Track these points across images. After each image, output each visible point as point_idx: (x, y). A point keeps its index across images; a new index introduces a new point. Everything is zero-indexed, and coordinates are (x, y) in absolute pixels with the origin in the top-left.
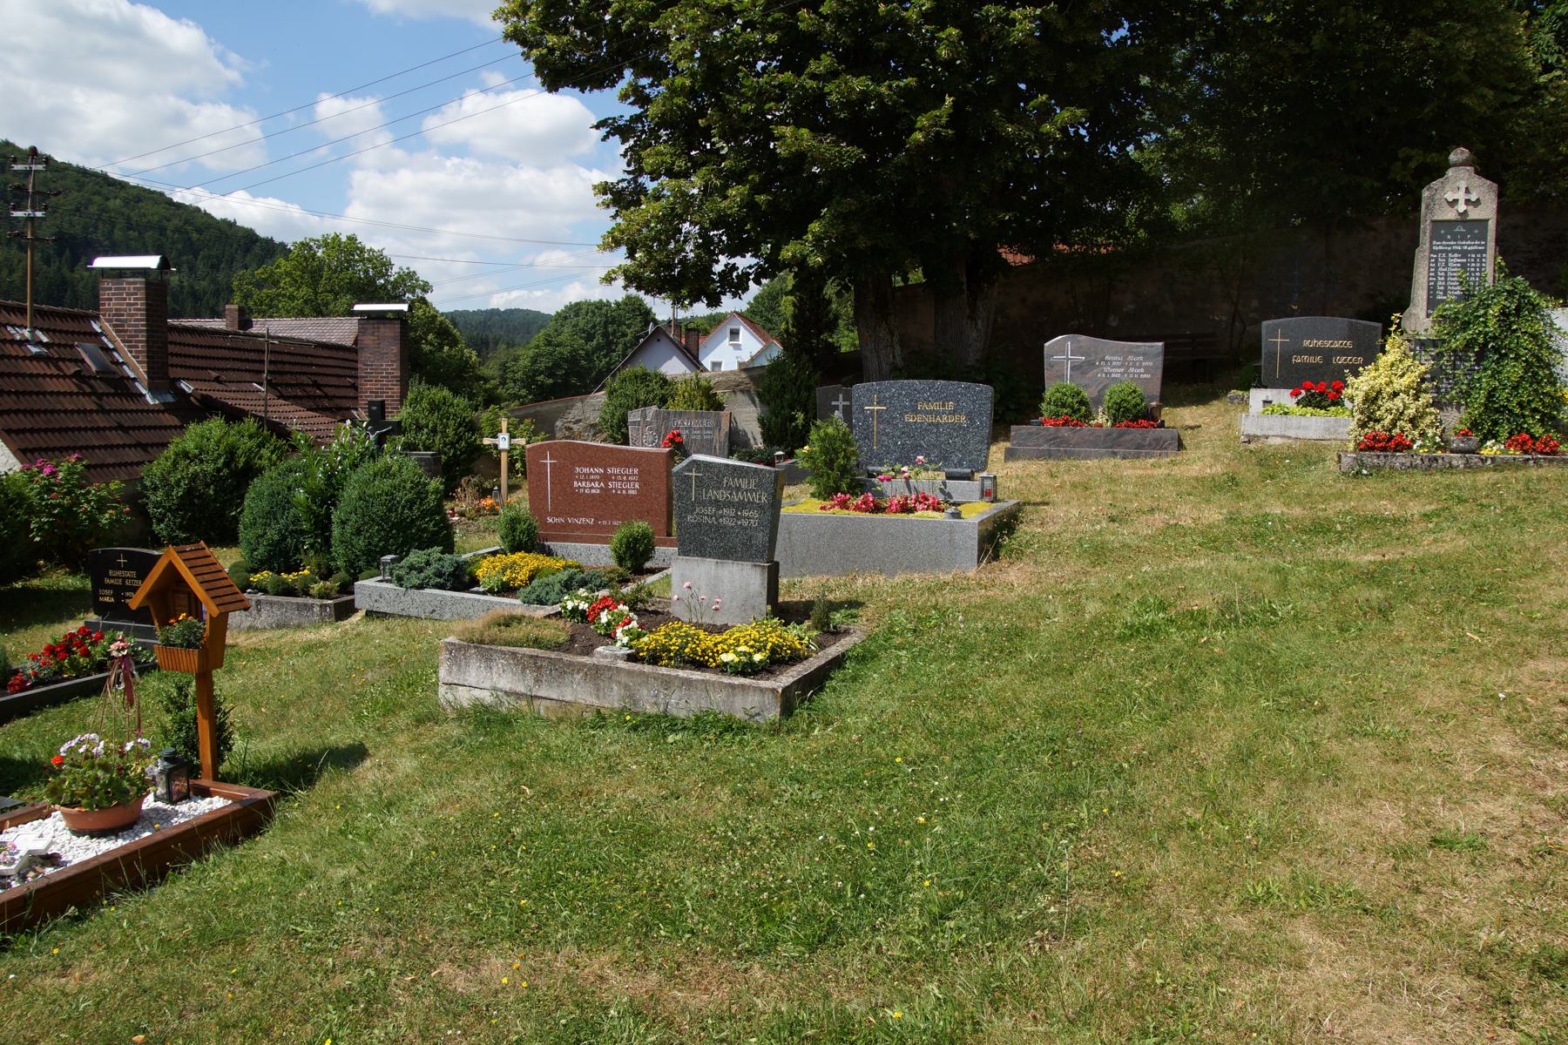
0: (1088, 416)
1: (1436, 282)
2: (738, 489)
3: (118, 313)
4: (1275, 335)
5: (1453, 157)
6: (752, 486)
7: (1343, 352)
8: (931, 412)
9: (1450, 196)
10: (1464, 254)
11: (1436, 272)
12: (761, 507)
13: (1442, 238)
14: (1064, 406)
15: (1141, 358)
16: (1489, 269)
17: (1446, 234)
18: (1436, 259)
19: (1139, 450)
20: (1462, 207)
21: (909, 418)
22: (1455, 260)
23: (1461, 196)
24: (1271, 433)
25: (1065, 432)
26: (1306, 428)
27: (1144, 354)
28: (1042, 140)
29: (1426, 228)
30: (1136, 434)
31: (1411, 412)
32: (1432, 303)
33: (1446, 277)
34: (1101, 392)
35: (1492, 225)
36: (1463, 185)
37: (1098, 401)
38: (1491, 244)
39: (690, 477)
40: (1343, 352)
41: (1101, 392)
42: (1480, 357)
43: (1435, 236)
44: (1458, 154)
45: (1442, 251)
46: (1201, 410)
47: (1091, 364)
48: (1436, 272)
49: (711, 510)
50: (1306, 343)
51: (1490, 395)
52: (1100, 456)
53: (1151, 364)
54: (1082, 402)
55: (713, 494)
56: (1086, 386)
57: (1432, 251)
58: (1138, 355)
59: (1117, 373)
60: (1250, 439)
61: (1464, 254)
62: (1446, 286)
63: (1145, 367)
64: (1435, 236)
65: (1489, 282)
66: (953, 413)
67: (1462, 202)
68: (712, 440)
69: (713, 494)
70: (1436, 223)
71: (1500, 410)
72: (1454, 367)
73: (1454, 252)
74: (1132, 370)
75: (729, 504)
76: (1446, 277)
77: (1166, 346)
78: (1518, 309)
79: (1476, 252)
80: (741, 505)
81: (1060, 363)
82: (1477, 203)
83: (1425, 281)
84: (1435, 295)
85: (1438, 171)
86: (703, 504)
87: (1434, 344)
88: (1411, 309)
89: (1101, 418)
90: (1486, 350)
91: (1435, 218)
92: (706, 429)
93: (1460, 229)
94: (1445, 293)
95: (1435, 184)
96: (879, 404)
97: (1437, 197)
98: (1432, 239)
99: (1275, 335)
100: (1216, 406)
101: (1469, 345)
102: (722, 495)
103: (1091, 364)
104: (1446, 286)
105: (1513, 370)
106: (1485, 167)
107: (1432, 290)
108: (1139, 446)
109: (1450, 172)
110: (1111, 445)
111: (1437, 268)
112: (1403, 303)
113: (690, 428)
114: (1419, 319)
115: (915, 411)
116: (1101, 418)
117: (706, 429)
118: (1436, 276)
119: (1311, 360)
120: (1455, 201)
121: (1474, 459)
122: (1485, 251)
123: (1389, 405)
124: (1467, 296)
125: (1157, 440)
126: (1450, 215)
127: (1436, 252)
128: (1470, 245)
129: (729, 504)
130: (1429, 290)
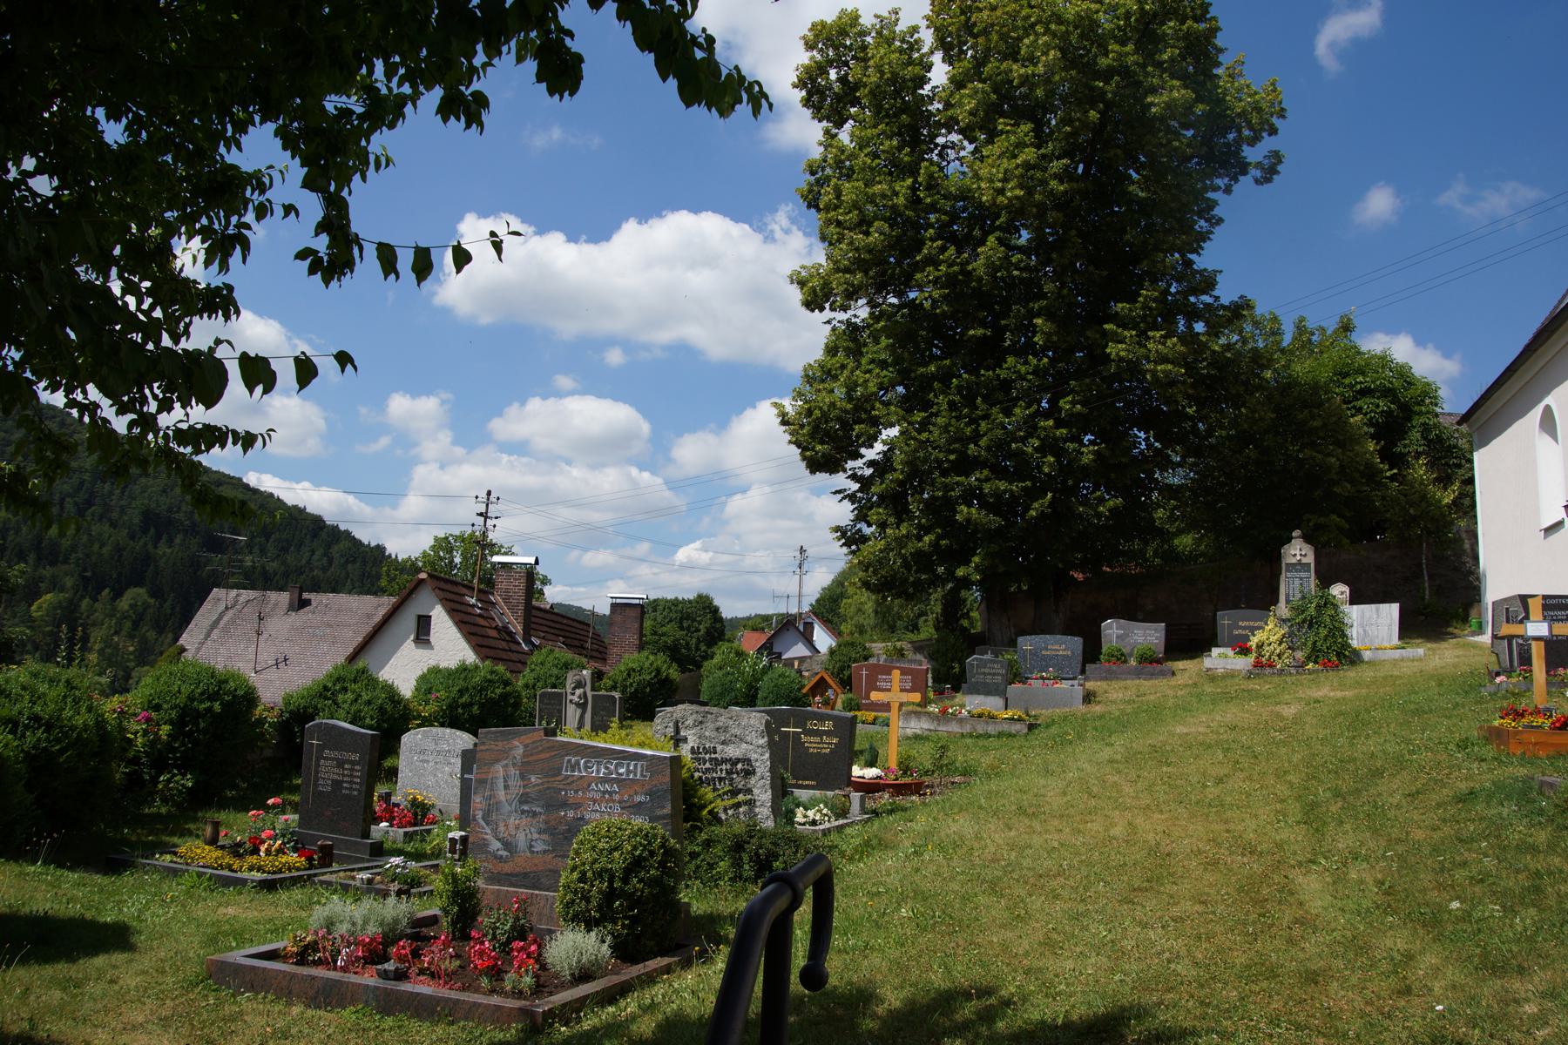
0: (1125, 662)
3: (507, 591)
4: (1224, 619)
5: (1294, 534)
10: (1301, 579)
14: (1113, 656)
16: (1313, 586)
19: (1152, 675)
20: (1298, 558)
21: (1043, 652)
22: (1297, 582)
23: (1298, 552)
25: (1114, 668)
27: (1155, 630)
28: (1099, 515)
29: (1283, 565)
30: (1149, 668)
31: (1278, 651)
32: (1288, 601)
34: (1132, 650)
35: (1313, 566)
37: (1131, 655)
38: (1313, 575)
41: (1132, 650)
42: (1310, 627)
43: (1287, 571)
44: (1296, 533)
46: (1189, 662)
47: (1127, 635)
49: (982, 677)
50: (1240, 623)
51: (1315, 643)
52: (1133, 679)
54: (1122, 655)
55: (983, 670)
56: (1125, 647)
58: (1150, 630)
59: (1140, 640)
60: (1208, 670)
61: (1301, 579)
64: (1287, 571)
65: (1313, 593)
69: (983, 670)
71: (1319, 651)
72: (1299, 631)
75: (990, 674)
77: (1166, 626)
78: (1325, 604)
80: (994, 674)
81: (1110, 635)
82: (1305, 555)
85: (1289, 540)
87: (1289, 620)
88: (1279, 605)
89: (1133, 662)
90: (1311, 623)
95: (1286, 547)
99: (1224, 619)
100: (1196, 661)
101: (1304, 621)
102: (987, 671)
103: (1127, 635)
105: (1323, 632)
106: (1307, 538)
107: (1287, 596)
108: (1152, 674)
110: (1138, 674)
112: (1276, 601)
114: (1282, 609)
115: (1047, 650)
116: (1133, 662)
120: (1295, 555)
121: (1300, 670)
123: (1267, 648)
124: (1303, 598)
125: (1161, 671)
126: (1293, 561)
128: (1303, 575)
129: (990, 674)
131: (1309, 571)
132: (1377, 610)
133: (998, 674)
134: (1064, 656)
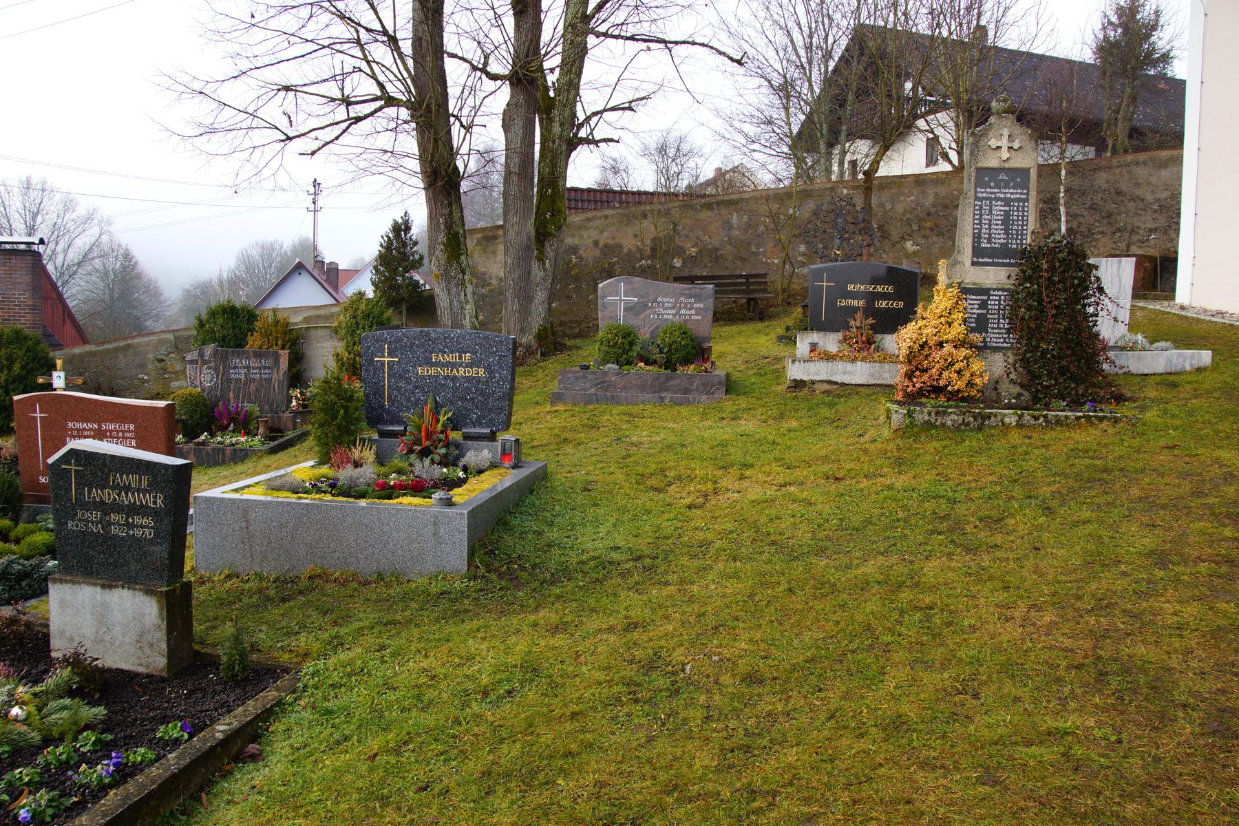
1: (980, 230)
2: (127, 489)
6: (144, 484)
7: (884, 296)
8: (448, 364)
9: (993, 143)
10: (1007, 202)
11: (980, 219)
12: (155, 513)
15: (693, 300)
17: (990, 181)
18: (981, 206)
20: (1005, 154)
22: (999, 208)
23: (1004, 143)
24: (818, 378)
26: (851, 373)
33: (990, 225)
36: (1006, 132)
38: (1033, 193)
39: (69, 471)
40: (884, 296)
43: (979, 183)
45: (986, 199)
47: (643, 307)
48: (980, 219)
49: (95, 515)
50: (850, 287)
53: (702, 306)
55: (97, 494)
57: (977, 198)
61: (1007, 202)
62: (990, 234)
63: (697, 309)
64: (979, 183)
66: (471, 365)
67: (1005, 149)
68: (270, 380)
70: (981, 171)
73: (997, 199)
74: (683, 311)
75: (116, 508)
76: (990, 225)
79: (1019, 200)
80: (133, 510)
81: (614, 304)
83: (970, 228)
84: (979, 243)
86: (86, 507)
91: (979, 165)
92: (265, 368)
93: (1003, 177)
94: (989, 241)
96: (390, 355)
97: (981, 143)
98: (976, 186)
102: (108, 495)
103: (645, 306)
104: (990, 234)
107: (977, 238)
109: (992, 119)
111: (981, 215)
113: (248, 367)
115: (430, 363)
117: (265, 368)
118: (980, 224)
120: (999, 148)
122: (1027, 200)
126: (993, 163)
127: (981, 199)
128: (1013, 193)
130: (974, 238)
131: (1025, 185)
132: (1120, 263)
133: (141, 510)
134: (469, 379)
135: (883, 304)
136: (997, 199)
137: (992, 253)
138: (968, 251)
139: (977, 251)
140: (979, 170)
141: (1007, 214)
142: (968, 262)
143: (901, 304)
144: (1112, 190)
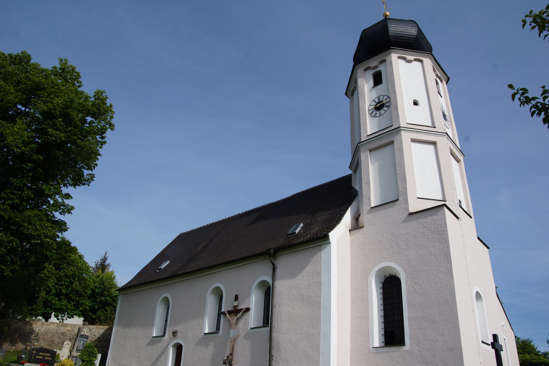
7: (47, 356)
9: (84, 330)
10: (84, 341)
13: (81, 338)
22: (82, 342)
23: (86, 330)
36: (86, 329)
40: (47, 356)
61: (84, 341)
64: (80, 337)
73: (82, 340)
79: (86, 341)
91: (81, 334)
107: (77, 347)
119: (40, 357)
126: (83, 333)
128: (85, 340)
135: (47, 358)
136: (82, 340)
137: (80, 350)
138: (75, 349)
139: (77, 350)
140: (80, 334)
141: (83, 343)
142: (75, 351)
143: (51, 359)
144: (93, 335)
